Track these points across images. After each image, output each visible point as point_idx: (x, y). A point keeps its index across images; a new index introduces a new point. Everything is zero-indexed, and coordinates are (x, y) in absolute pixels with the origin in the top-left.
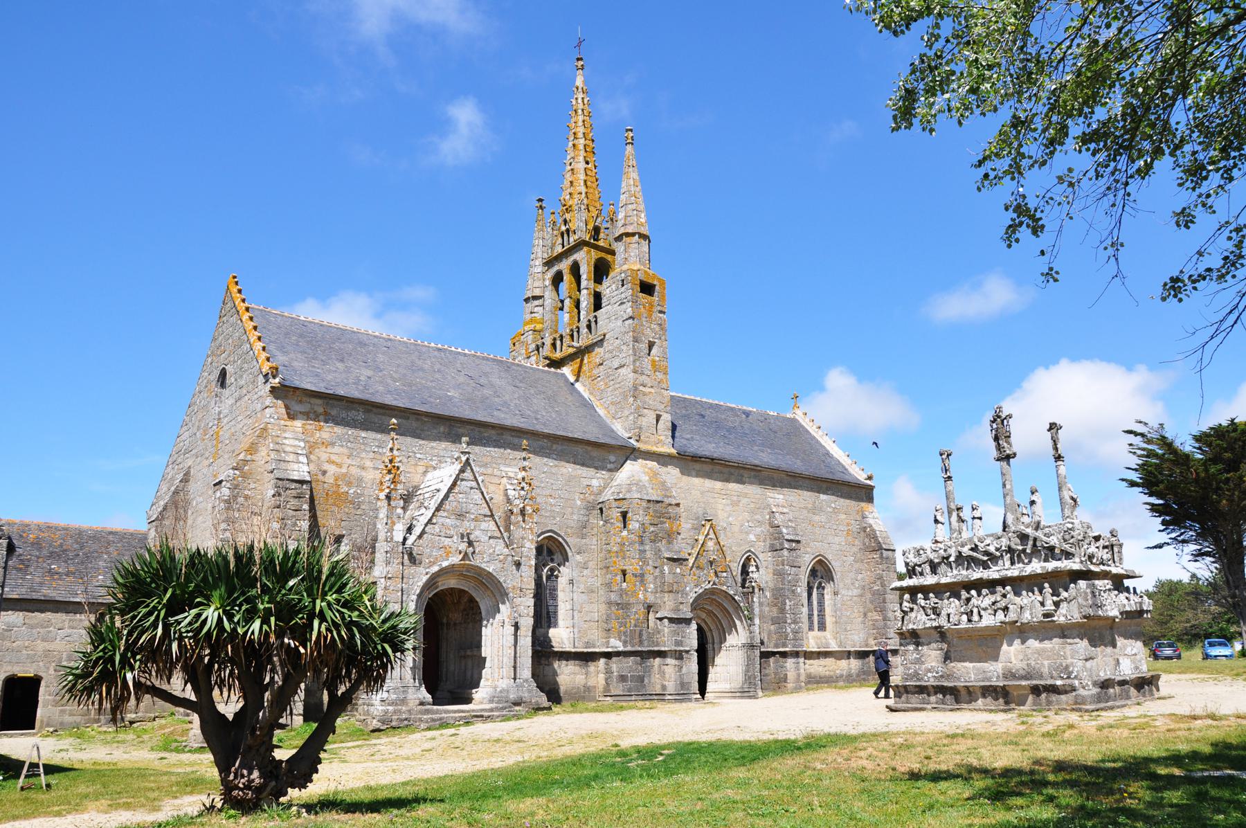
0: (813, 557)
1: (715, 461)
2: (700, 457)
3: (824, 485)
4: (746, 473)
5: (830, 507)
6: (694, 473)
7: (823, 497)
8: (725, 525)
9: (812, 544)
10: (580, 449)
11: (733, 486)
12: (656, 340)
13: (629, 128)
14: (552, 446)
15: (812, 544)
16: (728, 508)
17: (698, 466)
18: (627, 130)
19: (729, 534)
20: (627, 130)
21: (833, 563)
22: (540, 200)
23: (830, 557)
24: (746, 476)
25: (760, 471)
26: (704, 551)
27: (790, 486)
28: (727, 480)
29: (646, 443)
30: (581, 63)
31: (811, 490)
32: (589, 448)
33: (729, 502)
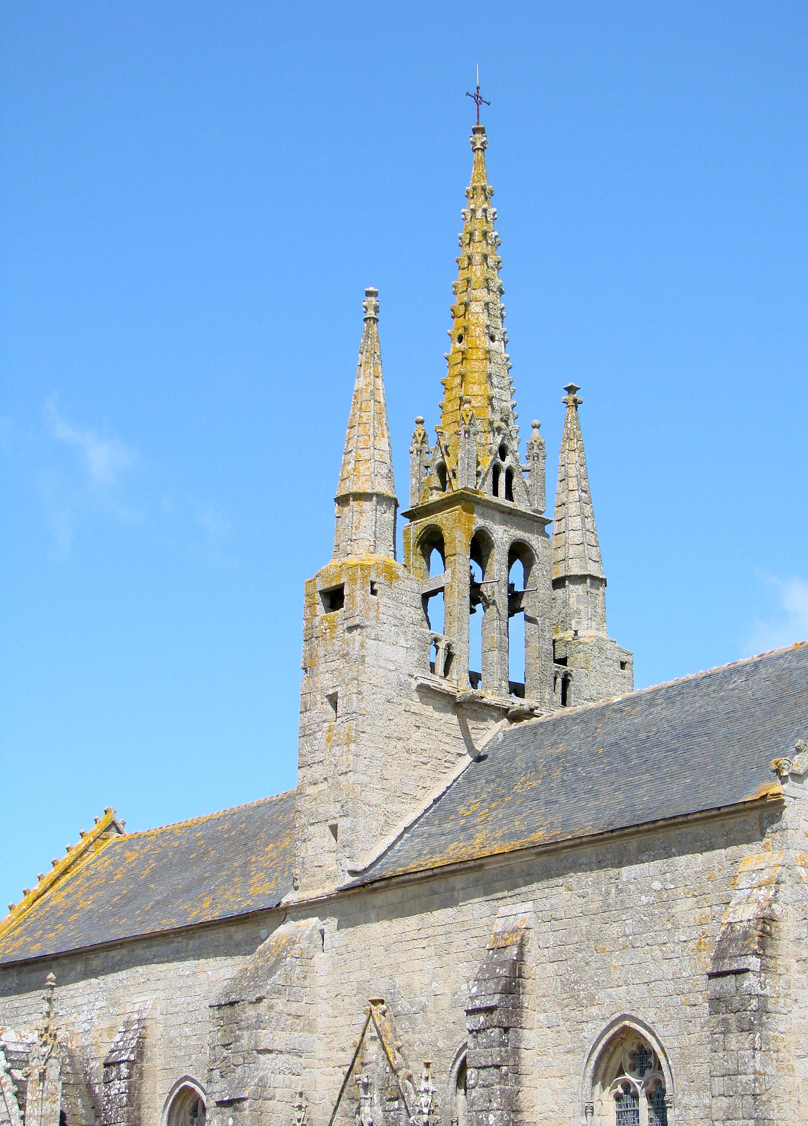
0: (604, 1025)
1: (722, 810)
2: (372, 883)
3: (633, 843)
4: (458, 882)
5: (648, 891)
6: (373, 915)
7: (628, 872)
8: (424, 999)
9: (601, 995)
10: (220, 935)
11: (441, 915)
12: (338, 689)
13: (371, 289)
14: (187, 945)
15: (601, 995)
16: (429, 965)
17: (379, 899)
18: (369, 294)
19: (432, 1017)
20: (369, 294)
21: (659, 1029)
22: (571, 390)
23: (649, 1016)
24: (458, 887)
25: (481, 866)
26: (363, 1064)
27: (548, 874)
28: (428, 908)
29: (307, 887)
30: (479, 139)
31: (600, 865)
32: (233, 929)
33: (431, 951)
